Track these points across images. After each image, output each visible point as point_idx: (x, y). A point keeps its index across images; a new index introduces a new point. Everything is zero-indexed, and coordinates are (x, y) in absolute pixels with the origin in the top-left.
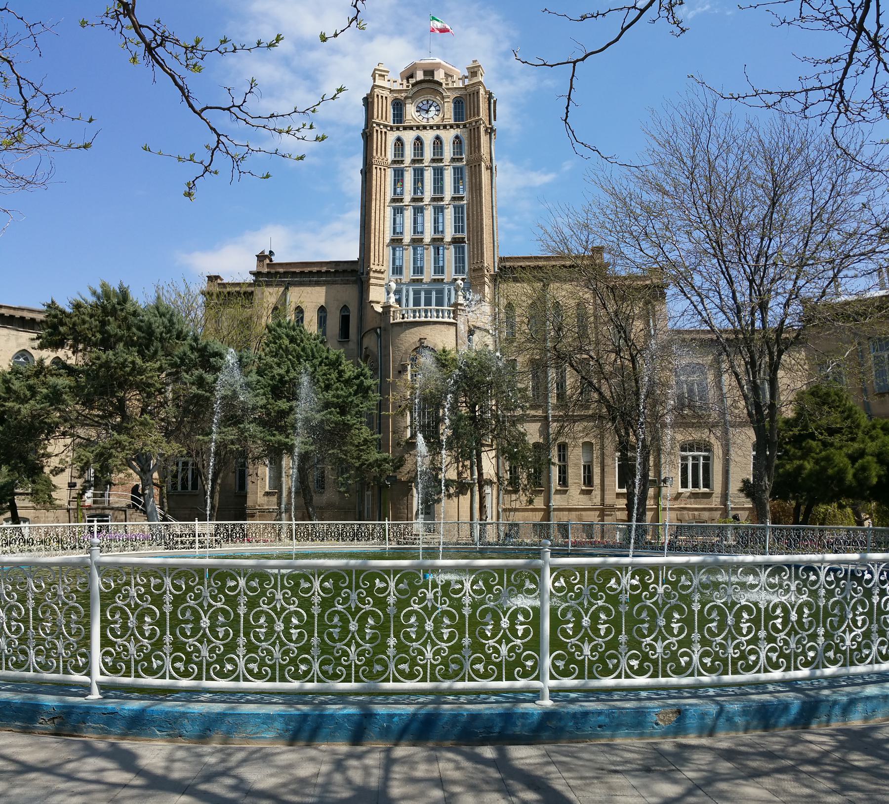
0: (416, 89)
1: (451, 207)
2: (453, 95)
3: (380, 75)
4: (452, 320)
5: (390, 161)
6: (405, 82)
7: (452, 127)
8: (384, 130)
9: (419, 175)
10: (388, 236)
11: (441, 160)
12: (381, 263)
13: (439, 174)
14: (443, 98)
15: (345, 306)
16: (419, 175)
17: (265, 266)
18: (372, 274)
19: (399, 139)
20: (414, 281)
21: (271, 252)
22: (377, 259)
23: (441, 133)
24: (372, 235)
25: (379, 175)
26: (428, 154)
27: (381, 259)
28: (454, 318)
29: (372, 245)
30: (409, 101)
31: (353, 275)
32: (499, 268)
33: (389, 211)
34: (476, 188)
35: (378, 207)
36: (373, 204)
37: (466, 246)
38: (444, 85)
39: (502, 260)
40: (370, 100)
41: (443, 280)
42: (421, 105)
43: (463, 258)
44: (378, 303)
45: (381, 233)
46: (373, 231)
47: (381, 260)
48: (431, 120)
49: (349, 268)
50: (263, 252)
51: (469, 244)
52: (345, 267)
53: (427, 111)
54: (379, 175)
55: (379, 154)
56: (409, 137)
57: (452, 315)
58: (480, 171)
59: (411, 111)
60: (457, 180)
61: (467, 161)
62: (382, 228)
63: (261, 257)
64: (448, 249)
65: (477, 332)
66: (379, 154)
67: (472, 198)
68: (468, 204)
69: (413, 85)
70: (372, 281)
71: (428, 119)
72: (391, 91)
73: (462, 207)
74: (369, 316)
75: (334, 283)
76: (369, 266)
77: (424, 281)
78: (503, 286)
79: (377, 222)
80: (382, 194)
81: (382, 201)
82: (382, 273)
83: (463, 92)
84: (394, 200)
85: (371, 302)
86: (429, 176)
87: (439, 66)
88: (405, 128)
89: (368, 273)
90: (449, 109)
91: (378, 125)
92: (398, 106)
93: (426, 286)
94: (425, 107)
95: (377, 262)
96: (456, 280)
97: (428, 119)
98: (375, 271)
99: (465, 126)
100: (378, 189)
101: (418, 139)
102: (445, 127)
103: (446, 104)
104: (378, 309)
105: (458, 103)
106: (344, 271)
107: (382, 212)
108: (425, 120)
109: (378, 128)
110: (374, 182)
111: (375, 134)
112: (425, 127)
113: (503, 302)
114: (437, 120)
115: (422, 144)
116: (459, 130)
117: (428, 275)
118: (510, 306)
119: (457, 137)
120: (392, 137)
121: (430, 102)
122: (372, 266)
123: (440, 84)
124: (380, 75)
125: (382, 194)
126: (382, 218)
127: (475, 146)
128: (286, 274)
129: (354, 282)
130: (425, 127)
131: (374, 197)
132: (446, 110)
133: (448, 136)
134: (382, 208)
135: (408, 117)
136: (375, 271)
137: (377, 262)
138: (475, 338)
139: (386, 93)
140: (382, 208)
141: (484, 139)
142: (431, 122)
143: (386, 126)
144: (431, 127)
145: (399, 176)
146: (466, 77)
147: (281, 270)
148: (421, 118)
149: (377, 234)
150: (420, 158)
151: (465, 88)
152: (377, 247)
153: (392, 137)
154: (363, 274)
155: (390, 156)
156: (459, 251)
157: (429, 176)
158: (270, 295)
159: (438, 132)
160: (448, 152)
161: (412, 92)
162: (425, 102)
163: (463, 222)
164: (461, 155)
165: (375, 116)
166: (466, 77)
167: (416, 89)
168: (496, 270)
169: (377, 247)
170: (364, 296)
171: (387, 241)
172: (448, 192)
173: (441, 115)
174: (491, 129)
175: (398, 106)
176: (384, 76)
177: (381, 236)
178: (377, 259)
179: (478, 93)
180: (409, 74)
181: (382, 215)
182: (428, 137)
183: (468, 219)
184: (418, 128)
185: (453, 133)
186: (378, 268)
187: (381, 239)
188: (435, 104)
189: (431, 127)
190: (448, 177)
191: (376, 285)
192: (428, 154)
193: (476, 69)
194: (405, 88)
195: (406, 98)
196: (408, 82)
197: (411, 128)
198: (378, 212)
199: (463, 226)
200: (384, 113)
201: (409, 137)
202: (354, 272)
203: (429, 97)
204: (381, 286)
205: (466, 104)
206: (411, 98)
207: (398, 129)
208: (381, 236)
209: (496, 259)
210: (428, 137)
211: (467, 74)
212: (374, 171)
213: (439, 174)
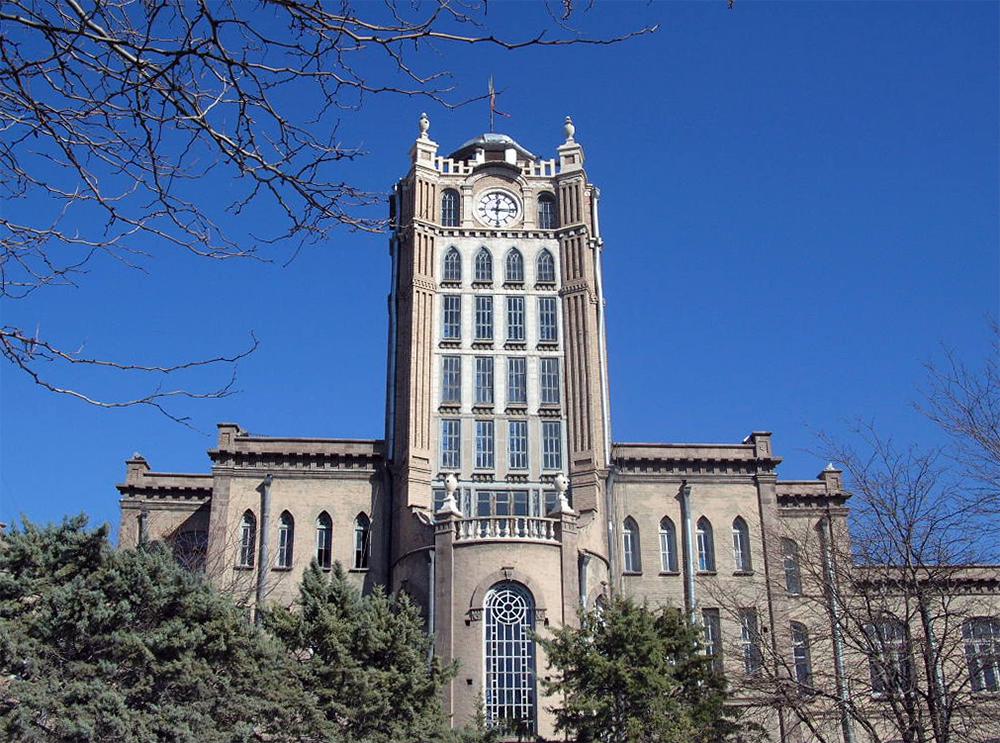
3: (423, 151)
4: (552, 541)
6: (461, 164)
7: (536, 235)
8: (430, 233)
24: (412, 399)
25: (422, 304)
26: (499, 274)
28: (555, 538)
29: (412, 415)
32: (612, 460)
36: (414, 350)
37: (564, 424)
38: (523, 173)
40: (405, 188)
41: (525, 476)
45: (426, 396)
48: (502, 223)
51: (568, 420)
54: (422, 304)
55: (423, 271)
57: (552, 533)
59: (474, 209)
60: (547, 318)
62: (426, 389)
65: (592, 563)
66: (423, 271)
70: (412, 474)
73: (556, 359)
74: (407, 531)
77: (496, 478)
78: (620, 488)
79: (420, 379)
84: (444, 344)
85: (412, 506)
89: (406, 461)
90: (531, 208)
96: (445, 475)
100: (421, 326)
108: (494, 223)
110: (415, 314)
111: (417, 238)
112: (494, 234)
114: (511, 224)
120: (442, 245)
128: (266, 457)
130: (494, 234)
131: (414, 338)
133: (530, 249)
138: (589, 570)
142: (503, 227)
144: (504, 235)
148: (486, 219)
159: (515, 243)
163: (556, 384)
168: (608, 463)
170: (396, 499)
173: (519, 217)
175: (453, 198)
177: (426, 401)
182: (500, 249)
184: (483, 234)
185: (537, 245)
187: (426, 406)
191: (418, 481)
192: (499, 274)
196: (466, 165)
197: (473, 234)
198: (420, 362)
200: (427, 207)
201: (469, 248)
204: (427, 483)
207: (451, 233)
208: (426, 401)
210: (500, 249)
212: (415, 296)
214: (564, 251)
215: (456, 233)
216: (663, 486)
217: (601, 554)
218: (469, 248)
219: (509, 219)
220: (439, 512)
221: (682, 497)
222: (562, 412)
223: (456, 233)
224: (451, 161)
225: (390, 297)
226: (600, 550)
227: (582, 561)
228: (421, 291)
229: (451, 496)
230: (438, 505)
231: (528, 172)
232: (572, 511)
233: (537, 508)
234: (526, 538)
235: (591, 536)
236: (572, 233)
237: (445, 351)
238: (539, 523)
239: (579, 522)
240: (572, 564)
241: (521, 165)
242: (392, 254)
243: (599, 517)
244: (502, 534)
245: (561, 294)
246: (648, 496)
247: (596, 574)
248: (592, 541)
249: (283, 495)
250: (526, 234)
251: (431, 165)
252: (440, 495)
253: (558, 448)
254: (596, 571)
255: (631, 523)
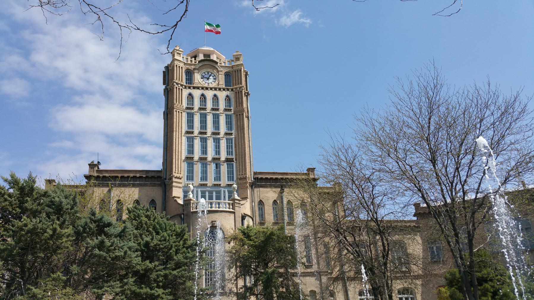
0: (201, 64)
1: (225, 139)
2: (225, 70)
3: (178, 53)
4: (231, 210)
5: (184, 107)
6: (193, 59)
7: (224, 90)
8: (181, 88)
9: (203, 119)
10: (184, 154)
11: (218, 110)
12: (179, 172)
13: (216, 118)
14: (218, 71)
15: (153, 200)
16: (203, 119)
17: (95, 172)
18: (174, 180)
19: (190, 94)
20: (202, 185)
21: (98, 162)
22: (177, 169)
23: (218, 93)
24: (174, 154)
25: (178, 116)
26: (209, 105)
27: (180, 169)
30: (196, 71)
31: (160, 180)
33: (184, 139)
34: (241, 129)
35: (177, 136)
36: (175, 134)
37: (234, 164)
38: (219, 64)
39: (255, 173)
40: (170, 68)
41: (220, 185)
42: (204, 74)
43: (233, 171)
44: (179, 198)
45: (180, 153)
46: (174, 151)
47: (179, 170)
49: (157, 175)
50: (93, 162)
51: (236, 163)
52: (153, 174)
53: (208, 79)
54: (178, 116)
56: (197, 94)
57: (231, 207)
58: (243, 118)
59: (197, 77)
61: (235, 112)
62: (180, 150)
63: (92, 166)
64: (223, 165)
65: (247, 218)
67: (238, 134)
68: (235, 138)
69: (199, 62)
70: (174, 184)
71: (208, 84)
72: (185, 64)
73: (232, 139)
75: (145, 185)
76: (172, 174)
77: (208, 185)
78: (256, 190)
79: (177, 146)
80: (180, 128)
81: (180, 132)
82: (180, 179)
83: (231, 69)
84: (187, 132)
85: (174, 197)
86: (210, 119)
87: (213, 53)
88: (194, 88)
89: (171, 179)
91: (177, 84)
92: (189, 74)
93: (209, 189)
94: (207, 76)
95: (177, 172)
97: (208, 84)
98: (176, 178)
99: (232, 90)
101: (203, 95)
102: (220, 89)
103: (220, 76)
104: (181, 202)
105: (227, 75)
106: (152, 177)
107: (180, 140)
108: (207, 84)
109: (177, 86)
110: (175, 120)
112: (207, 88)
113: (257, 200)
114: (214, 85)
115: (205, 98)
116: (229, 92)
117: (211, 181)
118: (261, 203)
119: (227, 96)
120: (185, 92)
121: (210, 73)
122: (174, 174)
123: (217, 63)
124: (178, 53)
125: (180, 128)
126: (180, 143)
127: (239, 103)
129: (160, 185)
130: (207, 88)
131: (175, 129)
132: (220, 79)
133: (222, 95)
134: (180, 137)
135: (196, 81)
136: (176, 178)
137: (177, 172)
139: (182, 65)
140: (180, 137)
141: (244, 99)
142: (211, 86)
143: (182, 85)
144: (211, 89)
145: (191, 117)
146: (232, 61)
147: (107, 175)
148: (204, 82)
149: (177, 153)
150: (204, 107)
151: (232, 67)
152: (177, 162)
153: (185, 92)
154: (166, 179)
155: (185, 104)
156: (230, 167)
157: (210, 119)
158: (99, 192)
159: (215, 92)
160: (222, 105)
161: (198, 66)
162: (206, 73)
164: (230, 107)
165: (175, 78)
166: (232, 61)
167: (201, 64)
169: (177, 162)
170: (167, 194)
171: (183, 158)
172: (223, 129)
173: (217, 82)
174: (248, 93)
175: (189, 74)
176: (180, 54)
177: (180, 155)
178: (177, 169)
179: (240, 70)
180: (194, 55)
181: (180, 141)
182: (209, 94)
183: (235, 147)
184: (203, 88)
186: (178, 175)
187: (180, 157)
188: (213, 75)
189: (211, 89)
190: (222, 120)
191: (176, 187)
192: (209, 105)
193: (239, 56)
194: (193, 63)
195: (194, 69)
196: (195, 60)
197: (198, 88)
198: (177, 139)
199: (232, 152)
200: (180, 77)
202: (159, 177)
203: (209, 70)
204: (180, 187)
205: (233, 77)
206: (198, 69)
207: (189, 88)
208: (180, 155)
209: (252, 173)
210: (209, 94)
211: (233, 59)
213: (216, 118)
214: (236, 97)
215: (192, 88)
216: (274, 189)
217: (250, 214)
218: (197, 94)
219: (213, 83)
220: (185, 199)
221: (282, 192)
222: (234, 160)
223: (192, 88)
224: (189, 58)
225: (164, 112)
226: (249, 213)
227: (243, 218)
228: (178, 111)
229: (191, 193)
230: (185, 196)
231: (221, 64)
232: (239, 198)
233: (224, 197)
234: (221, 209)
235: (246, 208)
236: (238, 89)
237: (187, 135)
238: (225, 203)
239: (242, 202)
240: (239, 219)
241: (218, 61)
242: (164, 95)
243: (248, 200)
244: (211, 207)
245: (234, 113)
246: (267, 192)
247: (248, 222)
248: (247, 210)
249: (117, 193)
250: (220, 89)
251: (180, 59)
252: (186, 193)
253: (233, 174)
254: (248, 221)
255: (261, 203)
